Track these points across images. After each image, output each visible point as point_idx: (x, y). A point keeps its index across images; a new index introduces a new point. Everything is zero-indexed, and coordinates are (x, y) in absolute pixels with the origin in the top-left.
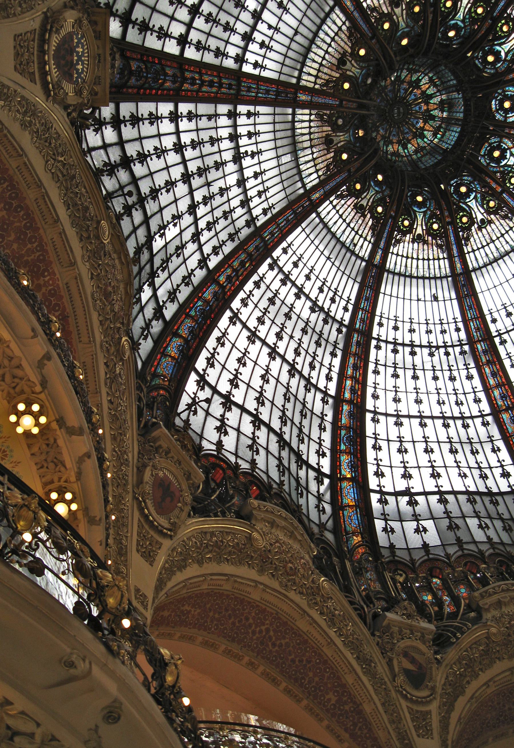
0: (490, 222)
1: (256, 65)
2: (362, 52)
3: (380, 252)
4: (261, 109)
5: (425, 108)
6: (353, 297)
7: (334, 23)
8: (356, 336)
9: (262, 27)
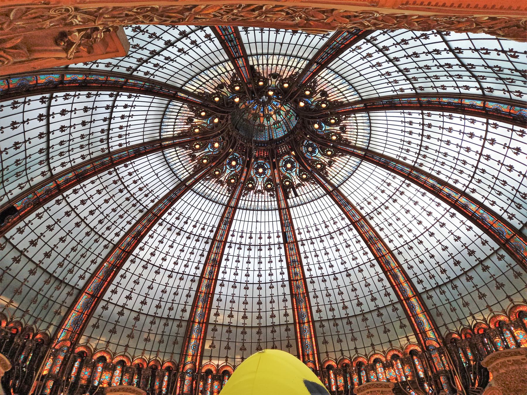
0: (223, 185)
2: (286, 85)
4: (216, 41)
5: (272, 113)
6: (131, 144)
7: (298, 63)
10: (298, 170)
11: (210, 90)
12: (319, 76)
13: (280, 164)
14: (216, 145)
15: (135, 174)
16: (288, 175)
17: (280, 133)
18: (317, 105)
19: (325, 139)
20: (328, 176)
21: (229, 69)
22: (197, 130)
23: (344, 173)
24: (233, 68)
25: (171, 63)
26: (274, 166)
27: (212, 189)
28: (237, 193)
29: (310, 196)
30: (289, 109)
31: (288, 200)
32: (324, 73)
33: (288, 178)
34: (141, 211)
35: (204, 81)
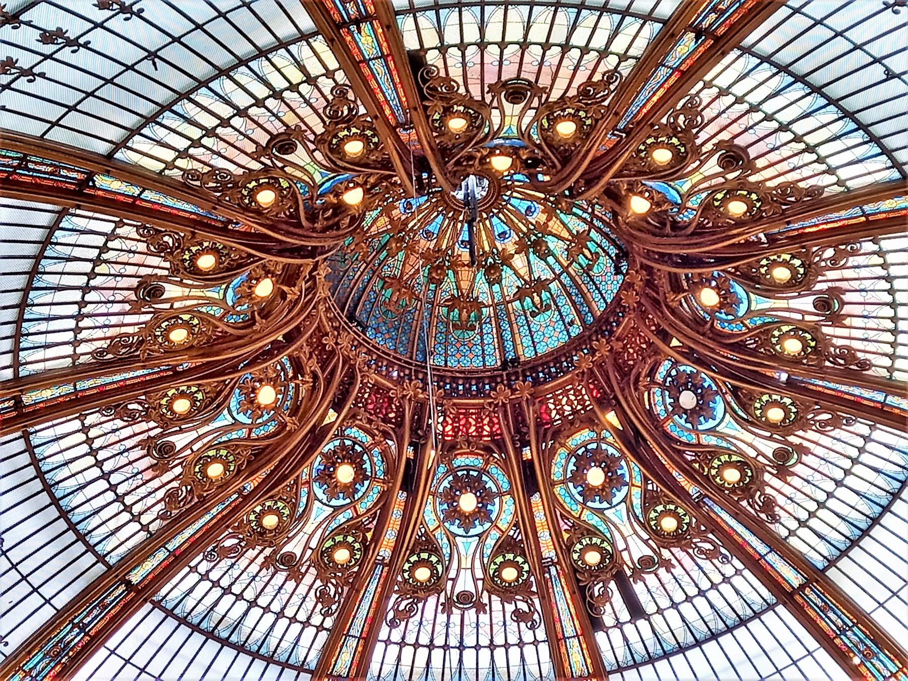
10: (636, 494)
11: (233, 157)
13: (557, 472)
14: (266, 395)
17: (548, 334)
18: (707, 208)
19: (754, 353)
20: (775, 519)
21: (315, 69)
22: (179, 336)
24: (332, 64)
27: (249, 595)
28: (364, 610)
29: (698, 614)
30: (583, 227)
31: (600, 637)
33: (592, 532)
35: (210, 122)
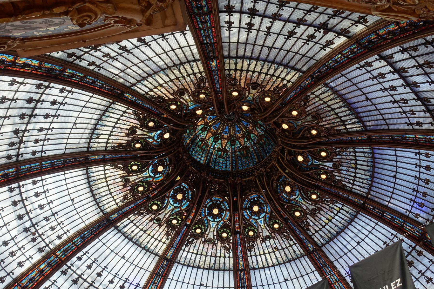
0: (160, 225)
1: (230, 23)
2: (267, 99)
3: (101, 157)
5: (239, 136)
6: (48, 153)
8: (12, 170)
9: (267, 22)
12: (313, 94)
15: (43, 196)
16: (253, 222)
23: (332, 228)
25: (125, 54)
26: (235, 208)
32: (320, 90)
34: (41, 250)
